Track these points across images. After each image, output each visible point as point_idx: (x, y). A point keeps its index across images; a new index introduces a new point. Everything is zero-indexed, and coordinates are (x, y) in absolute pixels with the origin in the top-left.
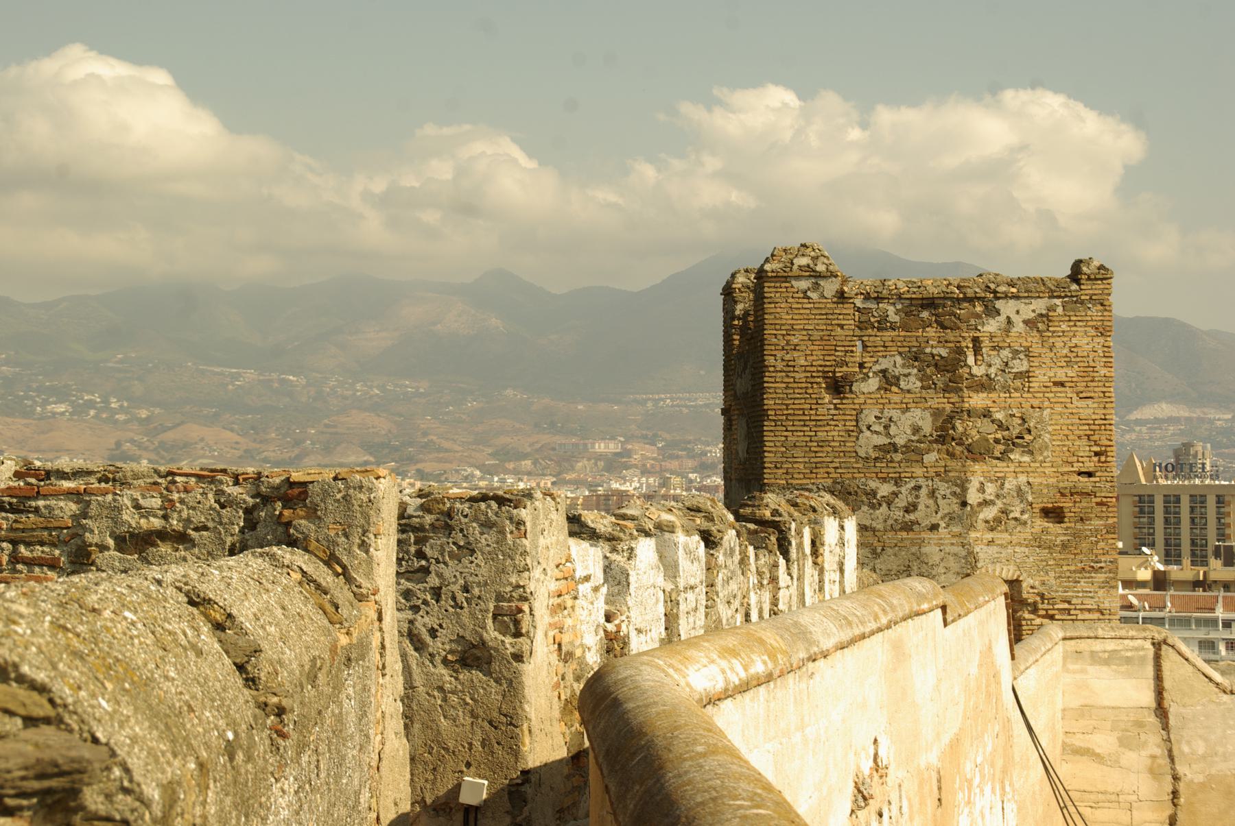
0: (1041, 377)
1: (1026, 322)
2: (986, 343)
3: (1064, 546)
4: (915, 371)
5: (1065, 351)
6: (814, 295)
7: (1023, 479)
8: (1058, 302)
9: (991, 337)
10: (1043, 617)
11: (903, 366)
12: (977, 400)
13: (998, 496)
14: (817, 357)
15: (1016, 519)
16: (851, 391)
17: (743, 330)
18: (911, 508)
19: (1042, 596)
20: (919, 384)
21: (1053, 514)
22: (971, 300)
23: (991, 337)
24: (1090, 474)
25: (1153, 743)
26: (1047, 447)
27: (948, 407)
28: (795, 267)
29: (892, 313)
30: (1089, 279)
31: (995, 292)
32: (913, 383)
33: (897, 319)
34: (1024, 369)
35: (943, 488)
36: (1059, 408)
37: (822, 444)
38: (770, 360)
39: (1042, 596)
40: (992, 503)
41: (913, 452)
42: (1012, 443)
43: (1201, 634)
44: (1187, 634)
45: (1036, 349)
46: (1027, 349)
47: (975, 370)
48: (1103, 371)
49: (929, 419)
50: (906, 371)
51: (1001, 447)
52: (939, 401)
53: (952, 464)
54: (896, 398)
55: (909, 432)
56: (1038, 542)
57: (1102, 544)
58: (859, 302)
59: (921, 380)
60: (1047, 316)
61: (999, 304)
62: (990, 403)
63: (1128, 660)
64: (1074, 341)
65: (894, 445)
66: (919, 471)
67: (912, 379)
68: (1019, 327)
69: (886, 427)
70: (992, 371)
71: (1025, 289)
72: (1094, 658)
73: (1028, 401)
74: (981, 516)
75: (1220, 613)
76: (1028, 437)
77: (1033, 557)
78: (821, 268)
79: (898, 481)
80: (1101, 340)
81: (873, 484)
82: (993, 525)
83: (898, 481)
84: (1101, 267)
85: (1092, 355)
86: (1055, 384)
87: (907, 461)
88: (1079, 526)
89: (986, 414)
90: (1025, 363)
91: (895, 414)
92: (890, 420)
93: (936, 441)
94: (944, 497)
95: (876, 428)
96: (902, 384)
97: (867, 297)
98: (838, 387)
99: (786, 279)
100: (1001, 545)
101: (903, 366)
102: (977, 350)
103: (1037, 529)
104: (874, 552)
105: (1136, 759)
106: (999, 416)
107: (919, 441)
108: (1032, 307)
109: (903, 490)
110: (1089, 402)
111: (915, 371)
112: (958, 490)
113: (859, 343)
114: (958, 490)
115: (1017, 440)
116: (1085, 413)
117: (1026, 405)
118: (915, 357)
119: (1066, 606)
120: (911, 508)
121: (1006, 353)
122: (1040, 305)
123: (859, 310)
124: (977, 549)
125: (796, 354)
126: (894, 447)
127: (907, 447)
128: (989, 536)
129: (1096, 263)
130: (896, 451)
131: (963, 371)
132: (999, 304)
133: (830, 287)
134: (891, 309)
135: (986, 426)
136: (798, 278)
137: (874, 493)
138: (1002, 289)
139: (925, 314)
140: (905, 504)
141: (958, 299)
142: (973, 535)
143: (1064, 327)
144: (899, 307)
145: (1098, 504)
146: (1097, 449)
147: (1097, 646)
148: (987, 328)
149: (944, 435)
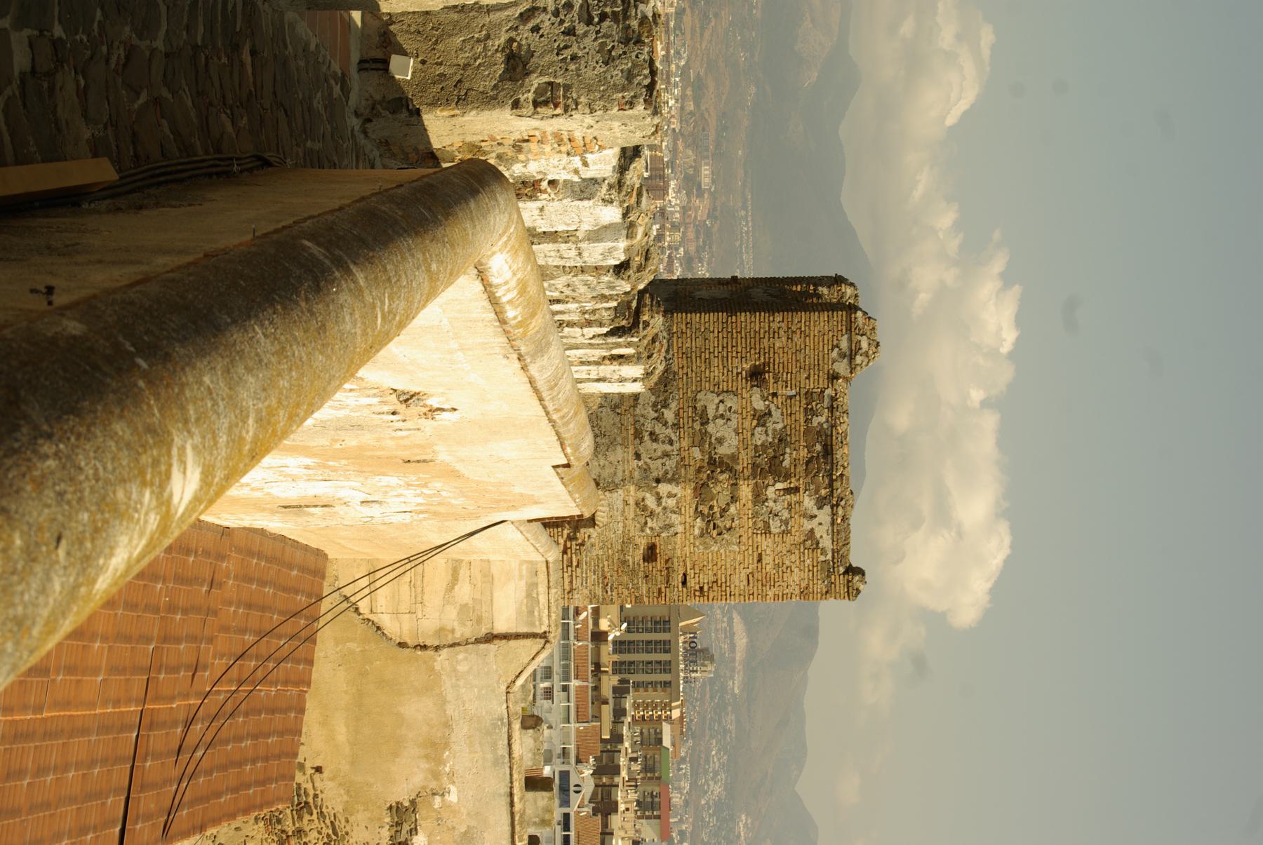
0: (766, 544)
1: (812, 531)
2: (794, 498)
3: (624, 562)
4: (770, 440)
5: (787, 563)
6: (835, 354)
7: (680, 529)
8: (829, 557)
9: (799, 503)
10: (565, 545)
11: (774, 430)
12: (745, 491)
13: (665, 508)
14: (781, 358)
15: (646, 523)
16: (752, 386)
17: (805, 294)
18: (654, 437)
19: (582, 544)
20: (759, 443)
21: (651, 554)
22: (831, 485)
23: (799, 503)
24: (684, 583)
25: (464, 631)
26: (706, 548)
27: (739, 468)
28: (859, 338)
29: (820, 420)
30: (849, 581)
31: (837, 505)
32: (760, 438)
33: (815, 424)
34: (773, 529)
35: (671, 464)
36: (739, 558)
37: (708, 362)
38: (778, 317)
39: (582, 544)
40: (659, 503)
41: (701, 439)
42: (709, 520)
43: (557, 669)
44: (556, 658)
45: (789, 539)
46: (789, 532)
47: (771, 490)
48: (771, 594)
49: (729, 452)
50: (770, 432)
51: (706, 511)
53: (692, 471)
54: (747, 424)
55: (719, 435)
56: (627, 541)
57: (626, 592)
58: (829, 392)
59: (762, 445)
60: (817, 548)
61: (827, 509)
62: (743, 502)
63: (531, 613)
64: (796, 570)
65: (707, 423)
66: (685, 443)
67: (763, 438)
68: (808, 525)
69: (722, 416)
70: (771, 504)
71: (840, 531)
72: (532, 586)
73: (746, 534)
74: (648, 495)
75: (574, 683)
76: (715, 533)
77: (615, 537)
78: (859, 359)
79: (676, 426)
80: (797, 592)
81: (673, 405)
83: (676, 426)
84: (858, 591)
85: (785, 584)
86: (760, 555)
87: (694, 434)
88: (641, 574)
89: (734, 499)
90: (778, 530)
91: (733, 423)
92: (729, 419)
93: (711, 458)
94: (663, 464)
95: (722, 407)
96: (759, 429)
97: (833, 399)
98: (757, 375)
99: (849, 330)
100: (624, 511)
101: (774, 430)
102: (788, 491)
103: (638, 541)
104: (616, 406)
106: (732, 509)
107: (710, 444)
108: (825, 535)
109: (669, 430)
110: (745, 583)
111: (770, 440)
112: (669, 476)
113: (793, 392)
114: (669, 476)
115: (713, 524)
116: (735, 579)
117: (742, 532)
118: (782, 440)
119: (575, 564)
120: (654, 437)
121: (785, 514)
122: (826, 542)
123: (822, 392)
124: (620, 492)
125: (784, 339)
126: (705, 423)
127: (705, 434)
128: (632, 502)
129: (862, 587)
130: (702, 424)
131: (770, 480)
132: (827, 509)
133: (842, 367)
134: (822, 419)
135: (724, 498)
136: (850, 339)
137: (666, 406)
138: (840, 511)
139: (818, 447)
140: (657, 432)
141: (831, 475)
142: (632, 488)
143: (808, 562)
144: (825, 426)
145: (660, 591)
146: (706, 588)
147: (542, 588)
148: (807, 499)
149: (716, 464)
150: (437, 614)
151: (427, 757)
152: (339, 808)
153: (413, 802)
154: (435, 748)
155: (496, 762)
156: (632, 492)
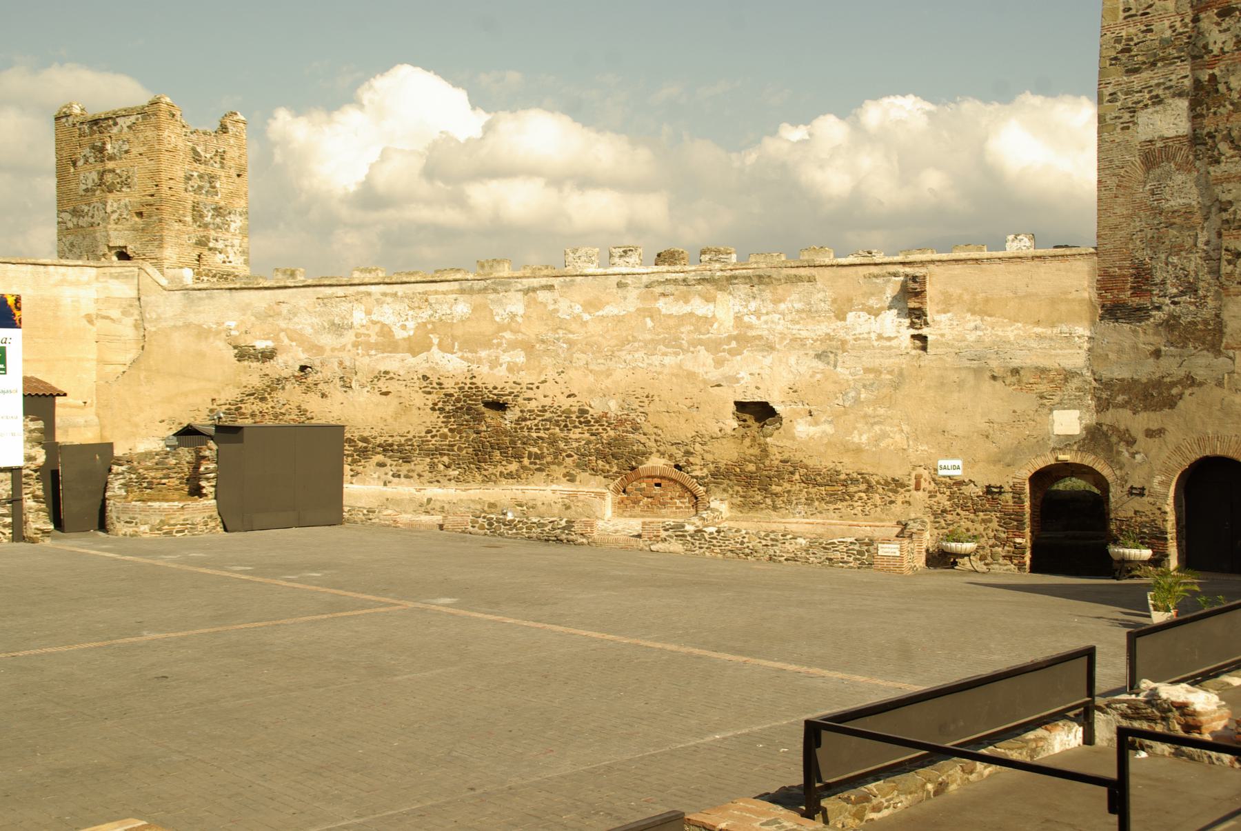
0: (134, 151)
3: (143, 230)
12: (110, 165)
21: (140, 214)
32: (92, 160)
52: (99, 167)
63: (127, 277)
68: (126, 129)
71: (127, 113)
72: (111, 276)
77: (130, 234)
82: (117, 222)
89: (113, 171)
105: (129, 321)
116: (151, 167)
118: (93, 147)
122: (133, 119)
147: (113, 270)
150: (127, 329)
151: (206, 338)
152: (238, 391)
153: (235, 347)
154: (203, 333)
155: (211, 298)
156: (112, 226)
